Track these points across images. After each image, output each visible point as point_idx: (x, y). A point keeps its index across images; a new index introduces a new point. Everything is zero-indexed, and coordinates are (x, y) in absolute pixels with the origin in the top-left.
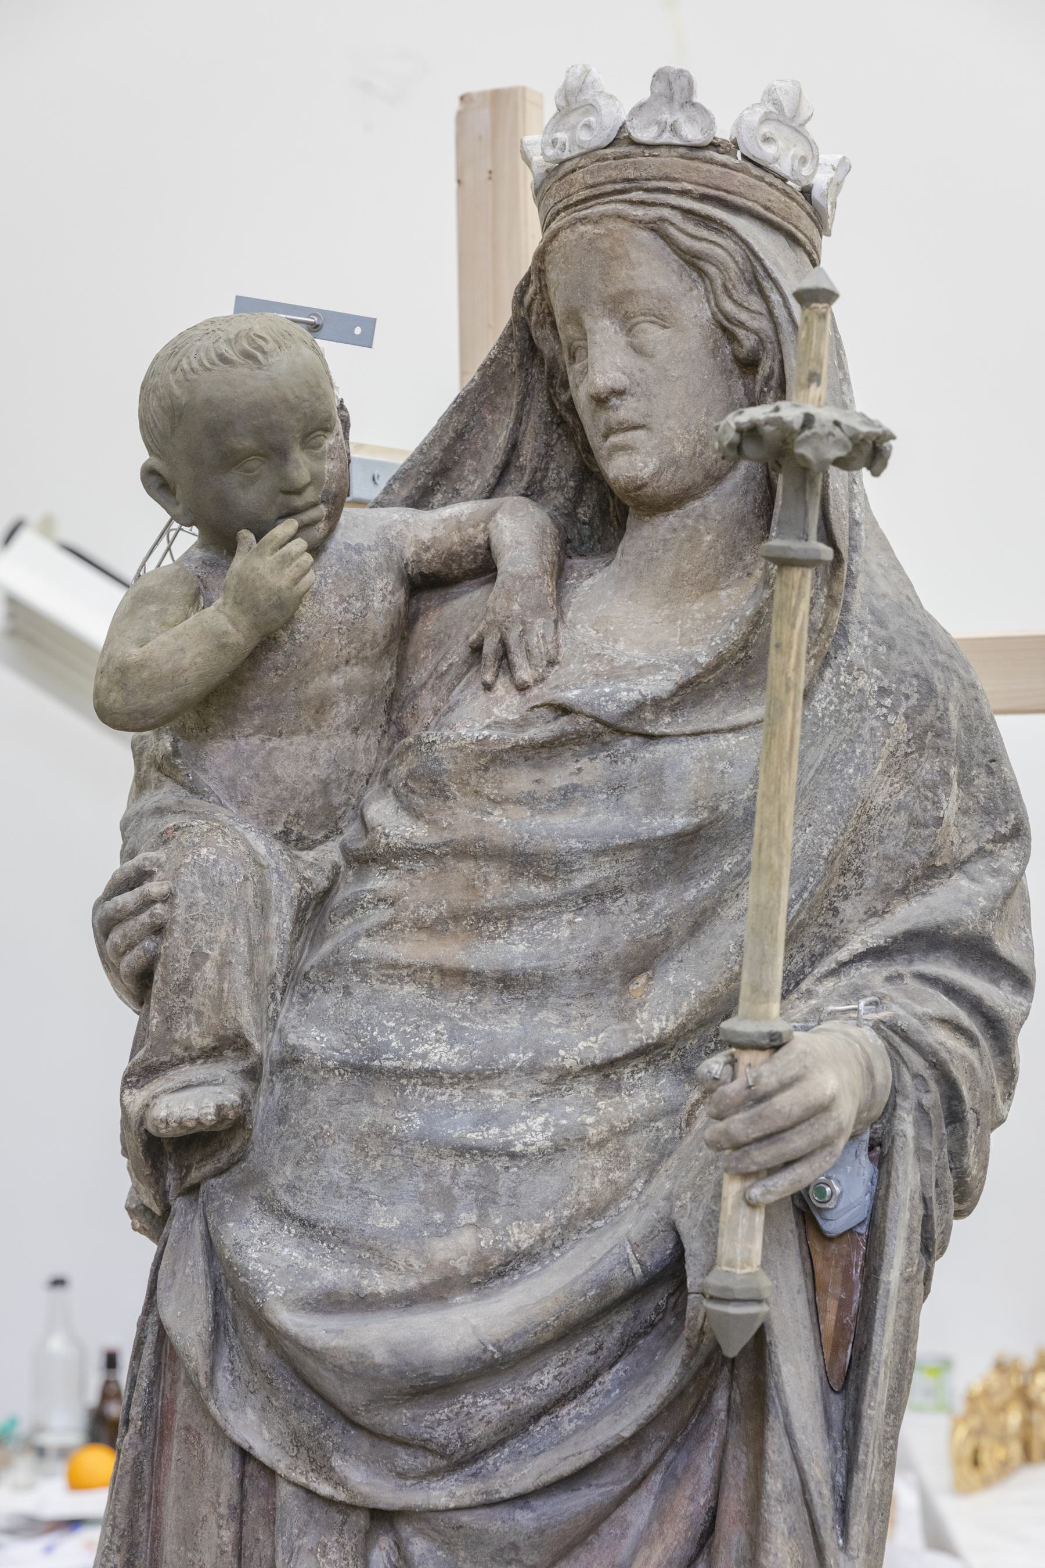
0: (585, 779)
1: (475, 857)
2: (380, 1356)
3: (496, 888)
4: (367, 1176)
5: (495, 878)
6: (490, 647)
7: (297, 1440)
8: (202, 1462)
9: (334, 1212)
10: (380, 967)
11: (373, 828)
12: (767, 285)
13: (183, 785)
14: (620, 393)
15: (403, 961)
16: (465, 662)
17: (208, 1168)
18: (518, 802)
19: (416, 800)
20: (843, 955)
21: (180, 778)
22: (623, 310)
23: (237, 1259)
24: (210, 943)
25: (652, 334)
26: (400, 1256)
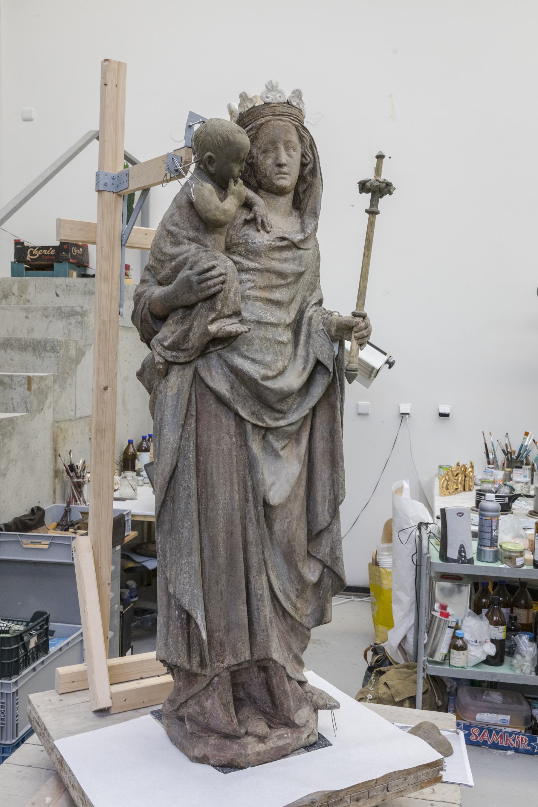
0: (289, 256)
1: (271, 272)
2: (286, 389)
3: (275, 281)
4: (263, 348)
5: (274, 278)
6: (259, 220)
7: (253, 413)
8: (221, 423)
9: (258, 357)
10: (253, 297)
11: (241, 263)
12: (314, 148)
13: (202, 245)
14: (285, 165)
15: (259, 296)
16: (243, 224)
17: (220, 347)
18: (277, 260)
19: (251, 257)
20: (313, 303)
21: (201, 243)
22: (288, 145)
23: (243, 368)
24: (232, 287)
25: (293, 153)
26: (273, 367)
